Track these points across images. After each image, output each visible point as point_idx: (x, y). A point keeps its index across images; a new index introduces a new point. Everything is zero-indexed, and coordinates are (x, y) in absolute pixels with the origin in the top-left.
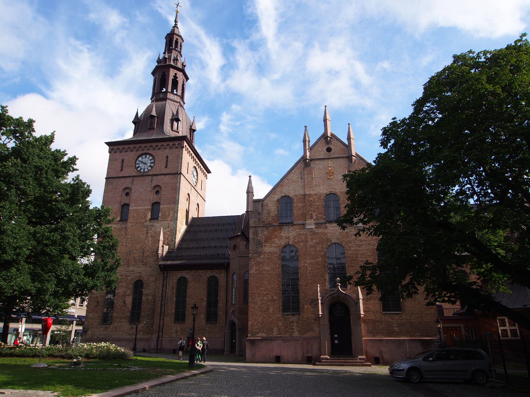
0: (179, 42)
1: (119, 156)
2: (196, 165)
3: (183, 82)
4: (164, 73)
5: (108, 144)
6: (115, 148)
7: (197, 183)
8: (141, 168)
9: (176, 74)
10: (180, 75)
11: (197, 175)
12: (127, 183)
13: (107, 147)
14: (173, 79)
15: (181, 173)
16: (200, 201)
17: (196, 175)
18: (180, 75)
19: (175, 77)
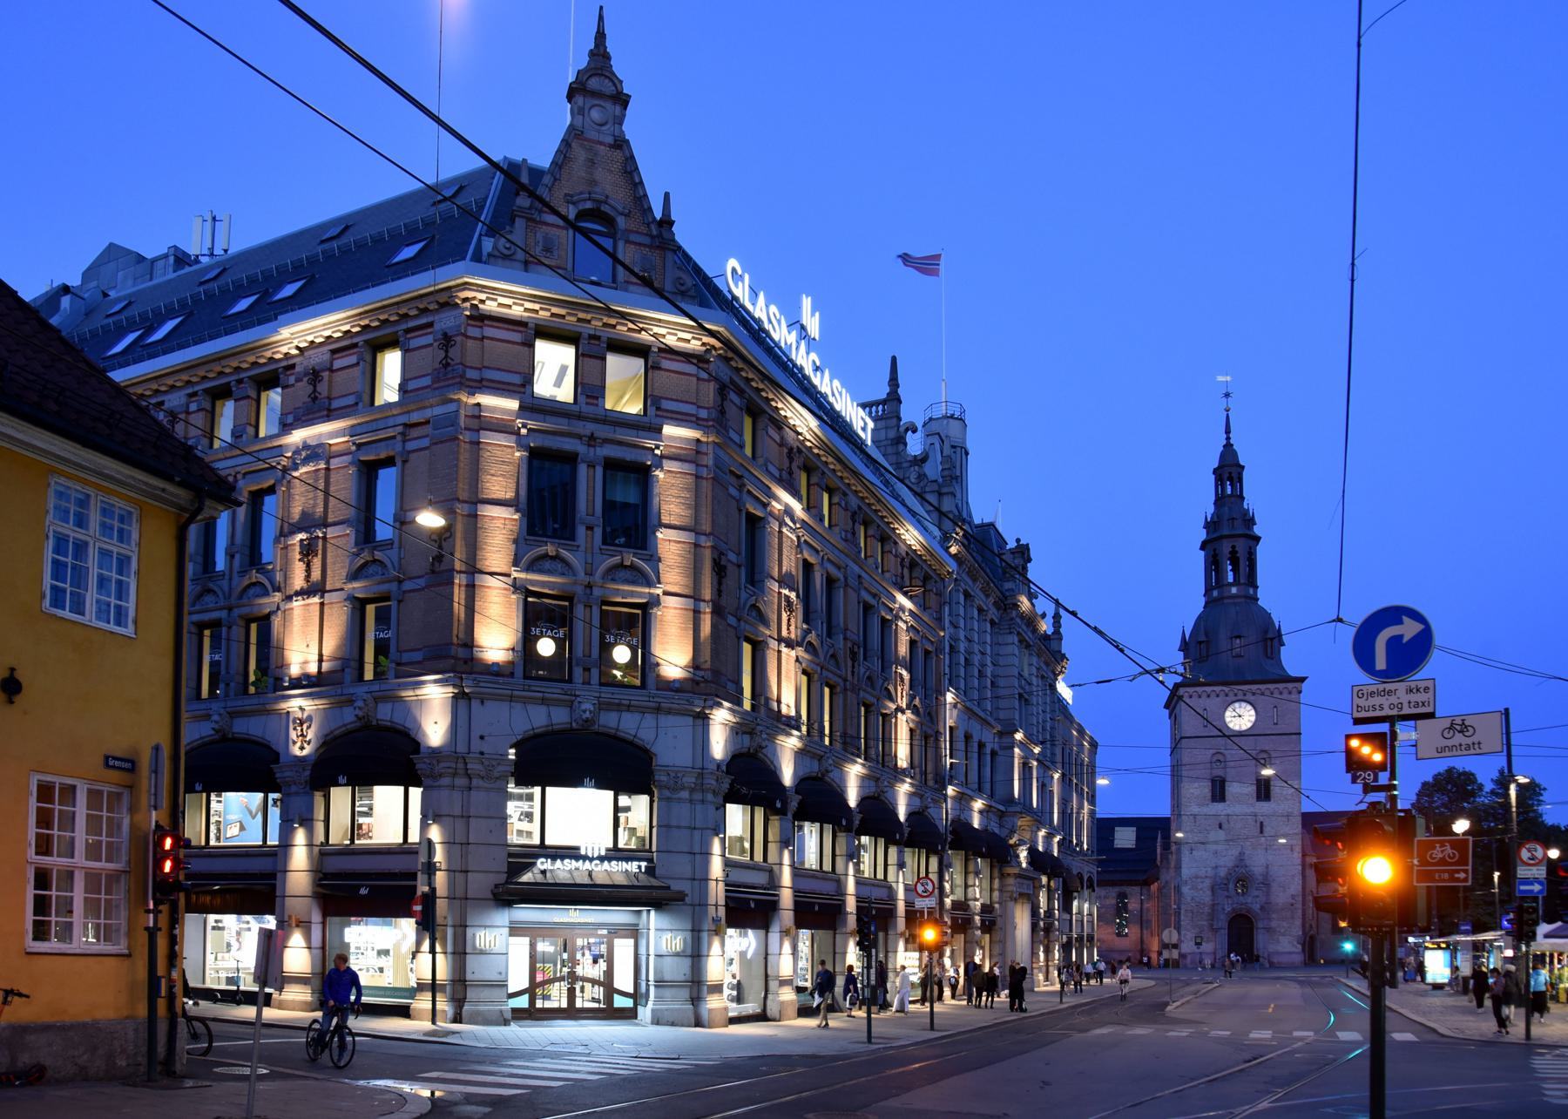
4: (1233, 547)
15: (1300, 734)
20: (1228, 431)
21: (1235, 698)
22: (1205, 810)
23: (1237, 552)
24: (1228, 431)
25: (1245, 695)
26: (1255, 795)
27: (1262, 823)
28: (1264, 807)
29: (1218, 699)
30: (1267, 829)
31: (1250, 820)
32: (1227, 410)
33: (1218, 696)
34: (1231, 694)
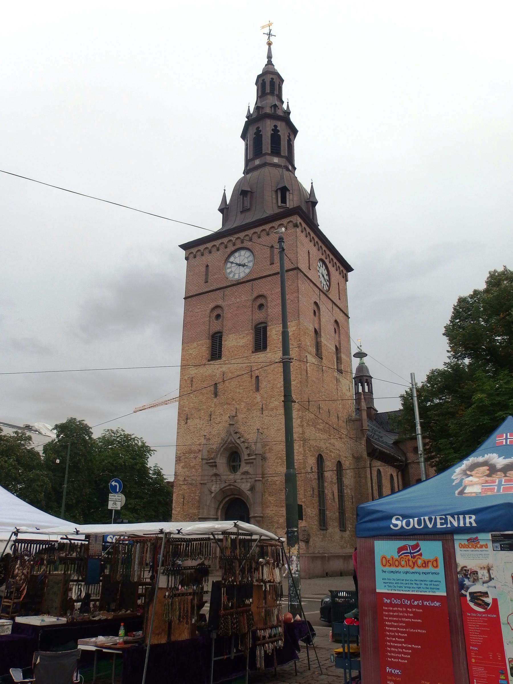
0: (276, 83)
1: (201, 261)
2: (323, 257)
3: (289, 137)
4: (258, 128)
5: (184, 247)
6: (194, 250)
7: (329, 287)
8: (235, 273)
9: (276, 126)
10: (281, 126)
11: (329, 274)
12: (217, 299)
13: (183, 252)
14: (272, 134)
15: (297, 268)
16: (341, 318)
17: (326, 273)
18: (281, 126)
19: (275, 130)
20: (269, 57)
21: (233, 248)
22: (202, 370)
23: (260, 131)
24: (269, 57)
25: (242, 242)
26: (251, 346)
27: (257, 377)
28: (261, 356)
29: (218, 253)
30: (263, 384)
31: (246, 377)
32: (269, 44)
33: (218, 250)
34: (230, 245)
